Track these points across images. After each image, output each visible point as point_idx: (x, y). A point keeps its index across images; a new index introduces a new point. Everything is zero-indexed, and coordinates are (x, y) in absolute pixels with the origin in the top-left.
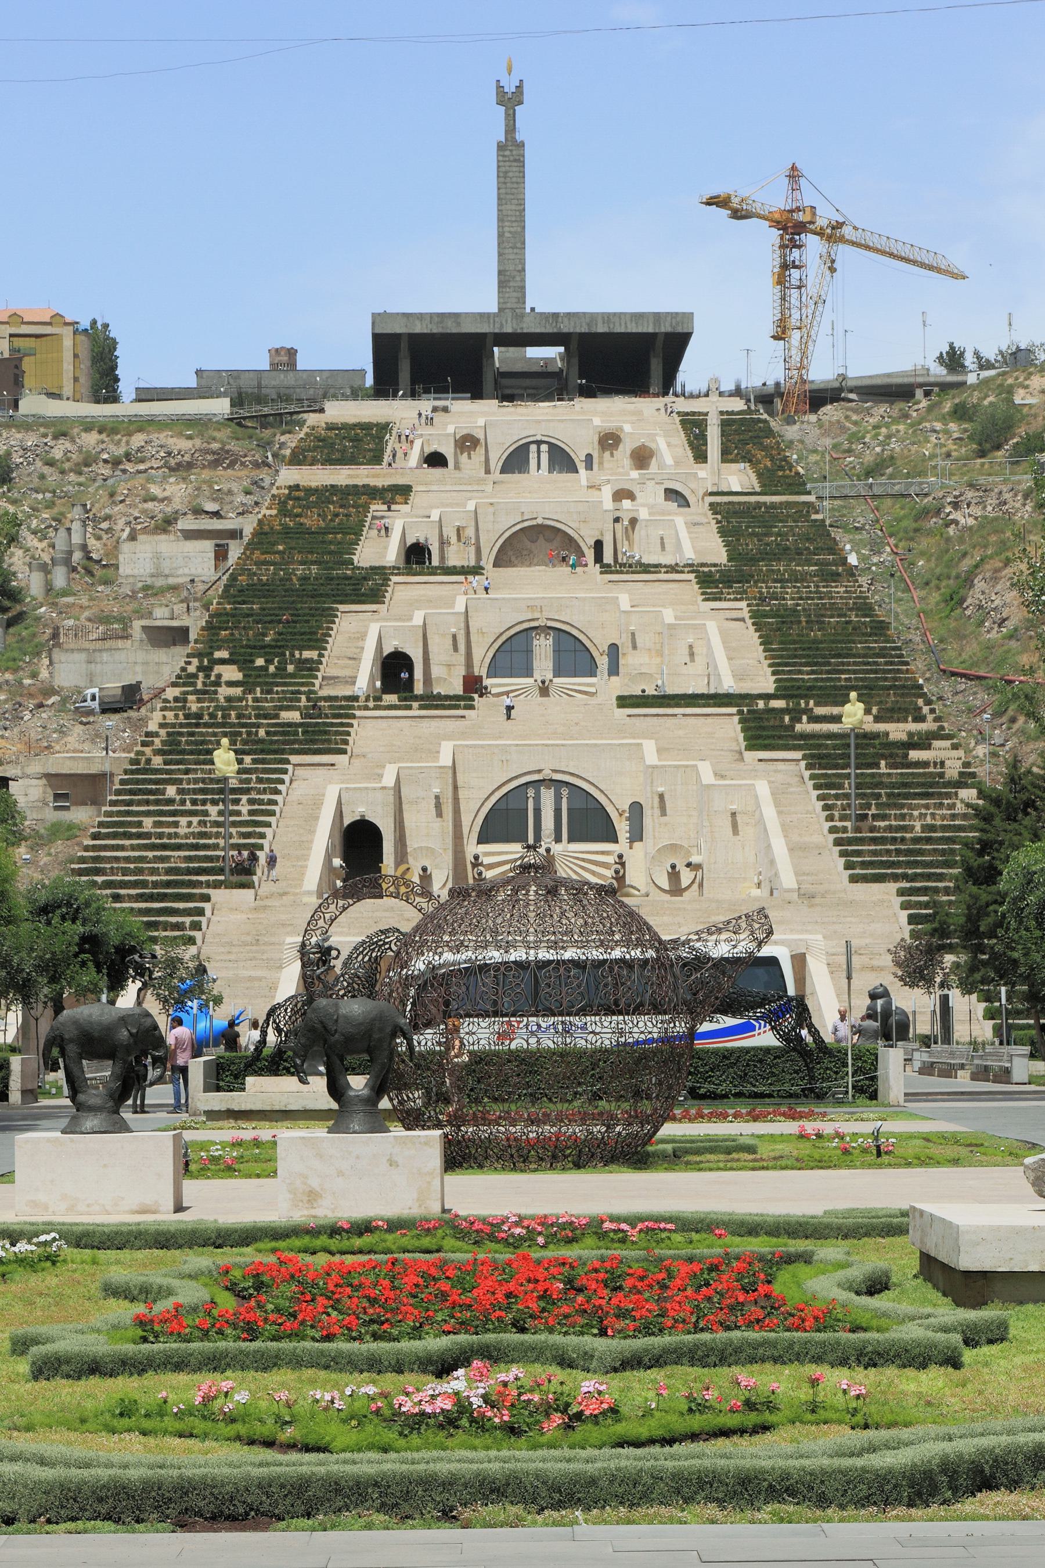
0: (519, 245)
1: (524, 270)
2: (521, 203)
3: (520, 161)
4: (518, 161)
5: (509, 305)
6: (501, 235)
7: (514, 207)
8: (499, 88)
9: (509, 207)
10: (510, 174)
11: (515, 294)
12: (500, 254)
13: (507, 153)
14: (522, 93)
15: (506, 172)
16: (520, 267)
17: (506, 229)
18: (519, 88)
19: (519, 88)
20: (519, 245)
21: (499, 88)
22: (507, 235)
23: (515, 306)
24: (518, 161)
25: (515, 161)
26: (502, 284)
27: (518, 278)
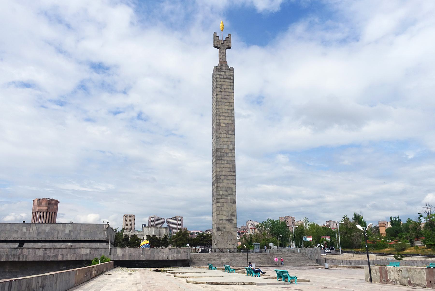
0: (230, 132)
1: (234, 149)
2: (232, 105)
3: (231, 79)
4: (230, 79)
5: (224, 173)
6: (218, 124)
7: (227, 107)
9: (223, 107)
10: (225, 87)
11: (228, 166)
12: (217, 138)
13: (222, 73)
14: (230, 41)
15: (221, 85)
16: (231, 147)
17: (221, 121)
22: (222, 125)
23: (228, 173)
25: (227, 78)
27: (230, 155)
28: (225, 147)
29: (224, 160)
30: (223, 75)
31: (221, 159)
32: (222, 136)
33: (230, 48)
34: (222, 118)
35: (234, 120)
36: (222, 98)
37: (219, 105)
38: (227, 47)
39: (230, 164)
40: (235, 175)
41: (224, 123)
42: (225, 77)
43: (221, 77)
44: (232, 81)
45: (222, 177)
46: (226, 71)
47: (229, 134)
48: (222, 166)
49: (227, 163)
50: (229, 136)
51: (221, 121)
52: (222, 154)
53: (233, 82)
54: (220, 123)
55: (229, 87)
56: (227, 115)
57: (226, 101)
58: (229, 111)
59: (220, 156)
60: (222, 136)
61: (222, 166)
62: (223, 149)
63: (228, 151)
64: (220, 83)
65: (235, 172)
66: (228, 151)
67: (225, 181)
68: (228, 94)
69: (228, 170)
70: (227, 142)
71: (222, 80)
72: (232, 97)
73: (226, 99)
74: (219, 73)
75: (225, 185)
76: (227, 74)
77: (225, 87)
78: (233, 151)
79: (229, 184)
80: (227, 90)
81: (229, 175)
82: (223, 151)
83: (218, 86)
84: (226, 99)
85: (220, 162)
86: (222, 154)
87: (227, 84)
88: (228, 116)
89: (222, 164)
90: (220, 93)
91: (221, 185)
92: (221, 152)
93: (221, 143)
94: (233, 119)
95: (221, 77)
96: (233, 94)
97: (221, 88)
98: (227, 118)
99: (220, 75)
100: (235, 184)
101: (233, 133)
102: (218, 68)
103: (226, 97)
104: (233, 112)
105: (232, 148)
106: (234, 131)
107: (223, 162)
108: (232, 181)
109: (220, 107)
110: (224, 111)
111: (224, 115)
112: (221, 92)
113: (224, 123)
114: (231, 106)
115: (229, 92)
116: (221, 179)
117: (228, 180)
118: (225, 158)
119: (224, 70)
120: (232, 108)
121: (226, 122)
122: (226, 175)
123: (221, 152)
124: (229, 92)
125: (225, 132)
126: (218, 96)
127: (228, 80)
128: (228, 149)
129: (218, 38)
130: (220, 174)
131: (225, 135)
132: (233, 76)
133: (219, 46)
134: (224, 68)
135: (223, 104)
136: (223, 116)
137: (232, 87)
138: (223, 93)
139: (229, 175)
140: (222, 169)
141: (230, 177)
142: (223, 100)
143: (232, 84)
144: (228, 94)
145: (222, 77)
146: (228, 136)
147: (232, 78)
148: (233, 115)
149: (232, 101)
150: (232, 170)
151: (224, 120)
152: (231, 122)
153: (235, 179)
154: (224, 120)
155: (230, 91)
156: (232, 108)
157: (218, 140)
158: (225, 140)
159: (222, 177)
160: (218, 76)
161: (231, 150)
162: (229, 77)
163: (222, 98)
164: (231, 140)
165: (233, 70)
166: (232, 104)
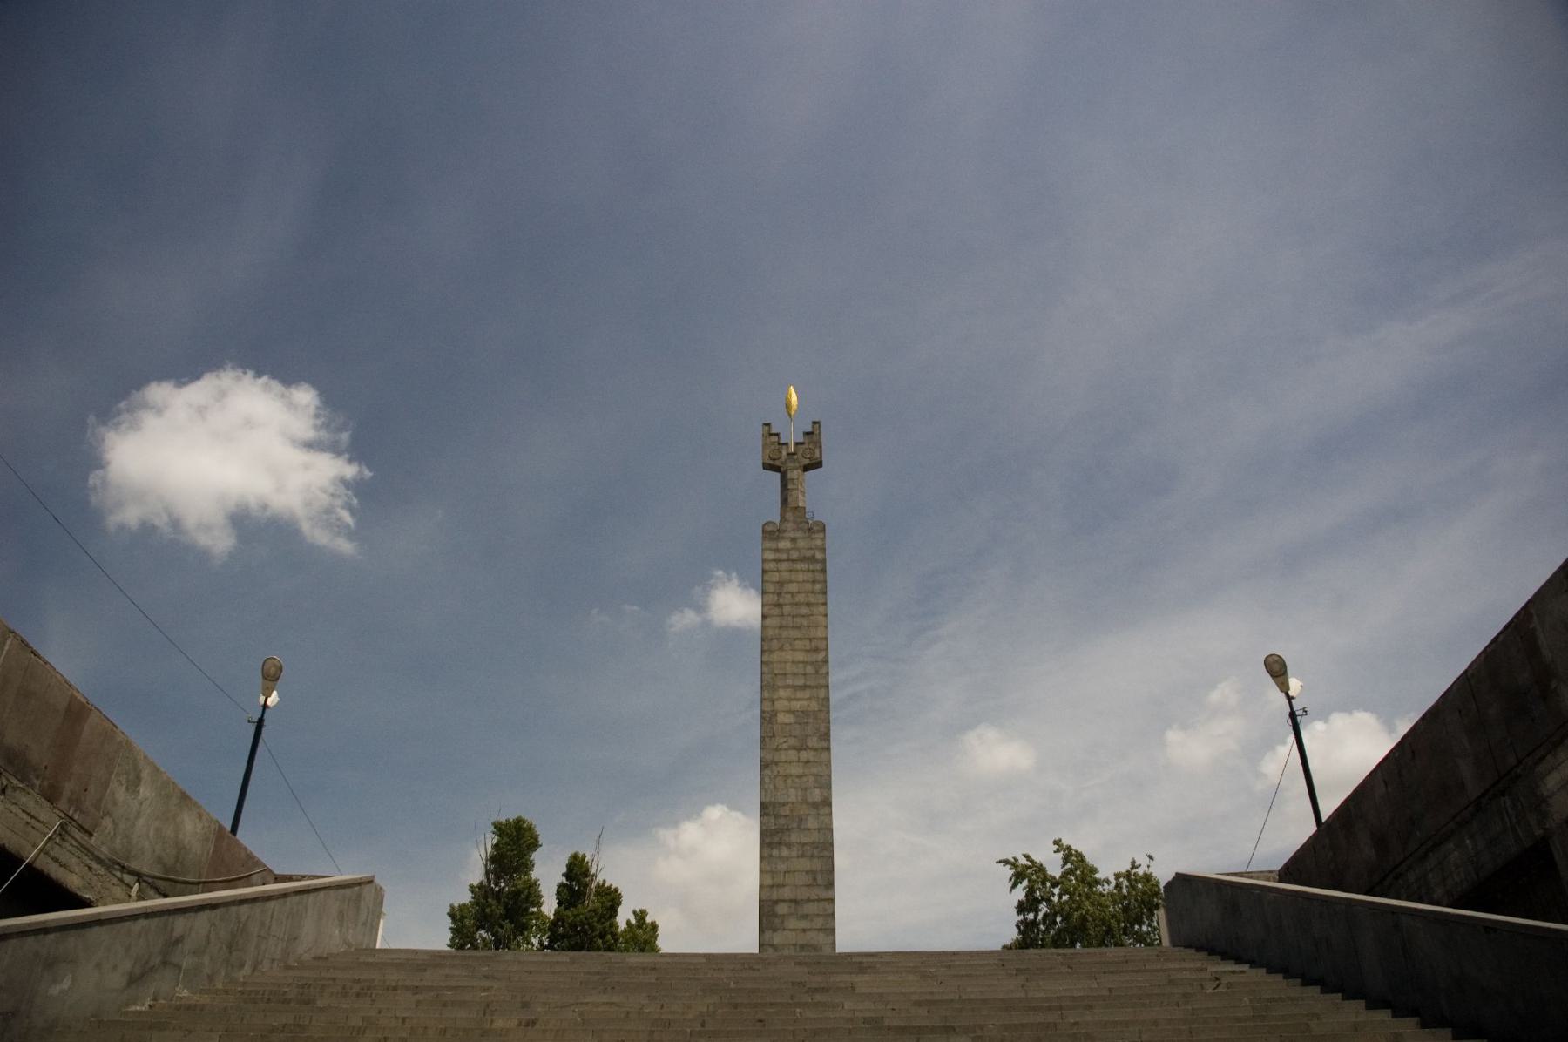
0: (813, 742)
1: (827, 803)
2: (819, 648)
3: (817, 564)
4: (812, 559)
5: (787, 893)
6: (768, 718)
7: (800, 656)
8: (769, 433)
9: (788, 656)
10: (793, 588)
11: (805, 864)
12: (765, 765)
13: (783, 544)
14: (819, 444)
15: (781, 583)
16: (816, 795)
17: (779, 705)
18: (813, 435)
19: (813, 435)
20: (813, 742)
21: (769, 433)
22: (782, 718)
23: (803, 894)
24: (812, 559)
26: (770, 840)
27: (811, 823)
28: (793, 795)
29: (789, 846)
30: (788, 550)
31: (776, 839)
32: (783, 757)
33: (818, 464)
34: (782, 693)
35: (827, 699)
36: (781, 627)
37: (771, 651)
38: (807, 462)
39: (812, 856)
40: (832, 900)
41: (790, 712)
42: (795, 555)
43: (778, 556)
44: (819, 566)
45: (782, 909)
46: (798, 534)
47: (807, 748)
48: (782, 867)
49: (803, 856)
50: (811, 755)
51: (779, 705)
52: (782, 821)
53: (824, 571)
54: (774, 714)
55: (808, 587)
56: (801, 682)
57: (796, 634)
58: (809, 669)
59: (776, 831)
60: (783, 757)
61: (782, 867)
62: (784, 804)
63: (804, 810)
64: (776, 577)
65: (830, 885)
66: (804, 810)
67: (792, 923)
68: (804, 610)
69: (802, 879)
70: (800, 777)
71: (784, 566)
72: (821, 618)
73: (799, 628)
74: (773, 545)
75: (792, 937)
76: (801, 543)
77: (793, 588)
78: (824, 811)
79: (810, 935)
80: (801, 598)
81: (809, 900)
82: (786, 811)
83: (770, 588)
84: (799, 628)
85: (775, 852)
86: (782, 821)
87: (801, 577)
88: (804, 687)
89: (780, 858)
90: (776, 611)
91: (777, 939)
92: (777, 816)
93: (780, 782)
94: (822, 693)
95: (778, 556)
96: (821, 609)
97: (779, 594)
98: (800, 694)
99: (777, 550)
100: (833, 930)
101: (824, 744)
102: (768, 528)
103: (798, 620)
104: (823, 671)
105: (818, 798)
106: (826, 736)
107: (785, 852)
108: (819, 923)
109: (775, 657)
110: (789, 668)
111: (789, 682)
112: (779, 605)
113: (790, 712)
114: (817, 650)
115: (808, 604)
116: (776, 916)
117: (805, 917)
118: (794, 838)
119: (792, 535)
120: (821, 656)
121: (797, 705)
122: (796, 902)
123: (777, 816)
124: (808, 604)
125: (792, 741)
126: (768, 622)
127: (804, 566)
128: (804, 801)
129: (775, 439)
130: (775, 897)
131: (793, 755)
132: (823, 550)
133: (778, 463)
134: (790, 526)
135: (787, 646)
136: (787, 687)
137: (818, 587)
138: (787, 609)
139: (809, 900)
140: (779, 880)
141: (810, 908)
142: (785, 633)
143: (819, 577)
144: (804, 610)
145: (784, 556)
146: (804, 756)
147: (819, 556)
148: (822, 682)
149: (820, 634)
150: (820, 881)
151: (790, 699)
152: (814, 706)
153: (833, 914)
154: (790, 699)
155: (812, 600)
156: (821, 656)
157: (767, 772)
158: (796, 770)
159: (782, 909)
160: (770, 555)
161: (815, 805)
162: (809, 554)
163: (781, 627)
164: (815, 770)
165: (824, 530)
166: (822, 645)
